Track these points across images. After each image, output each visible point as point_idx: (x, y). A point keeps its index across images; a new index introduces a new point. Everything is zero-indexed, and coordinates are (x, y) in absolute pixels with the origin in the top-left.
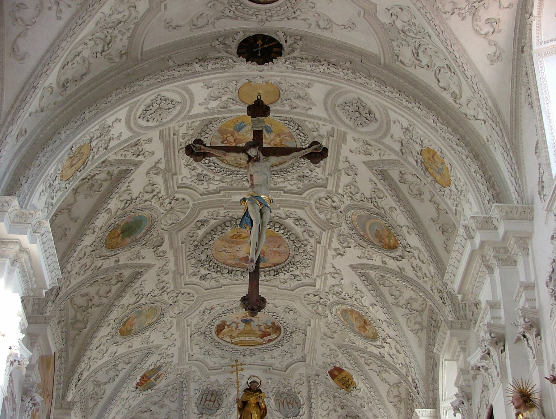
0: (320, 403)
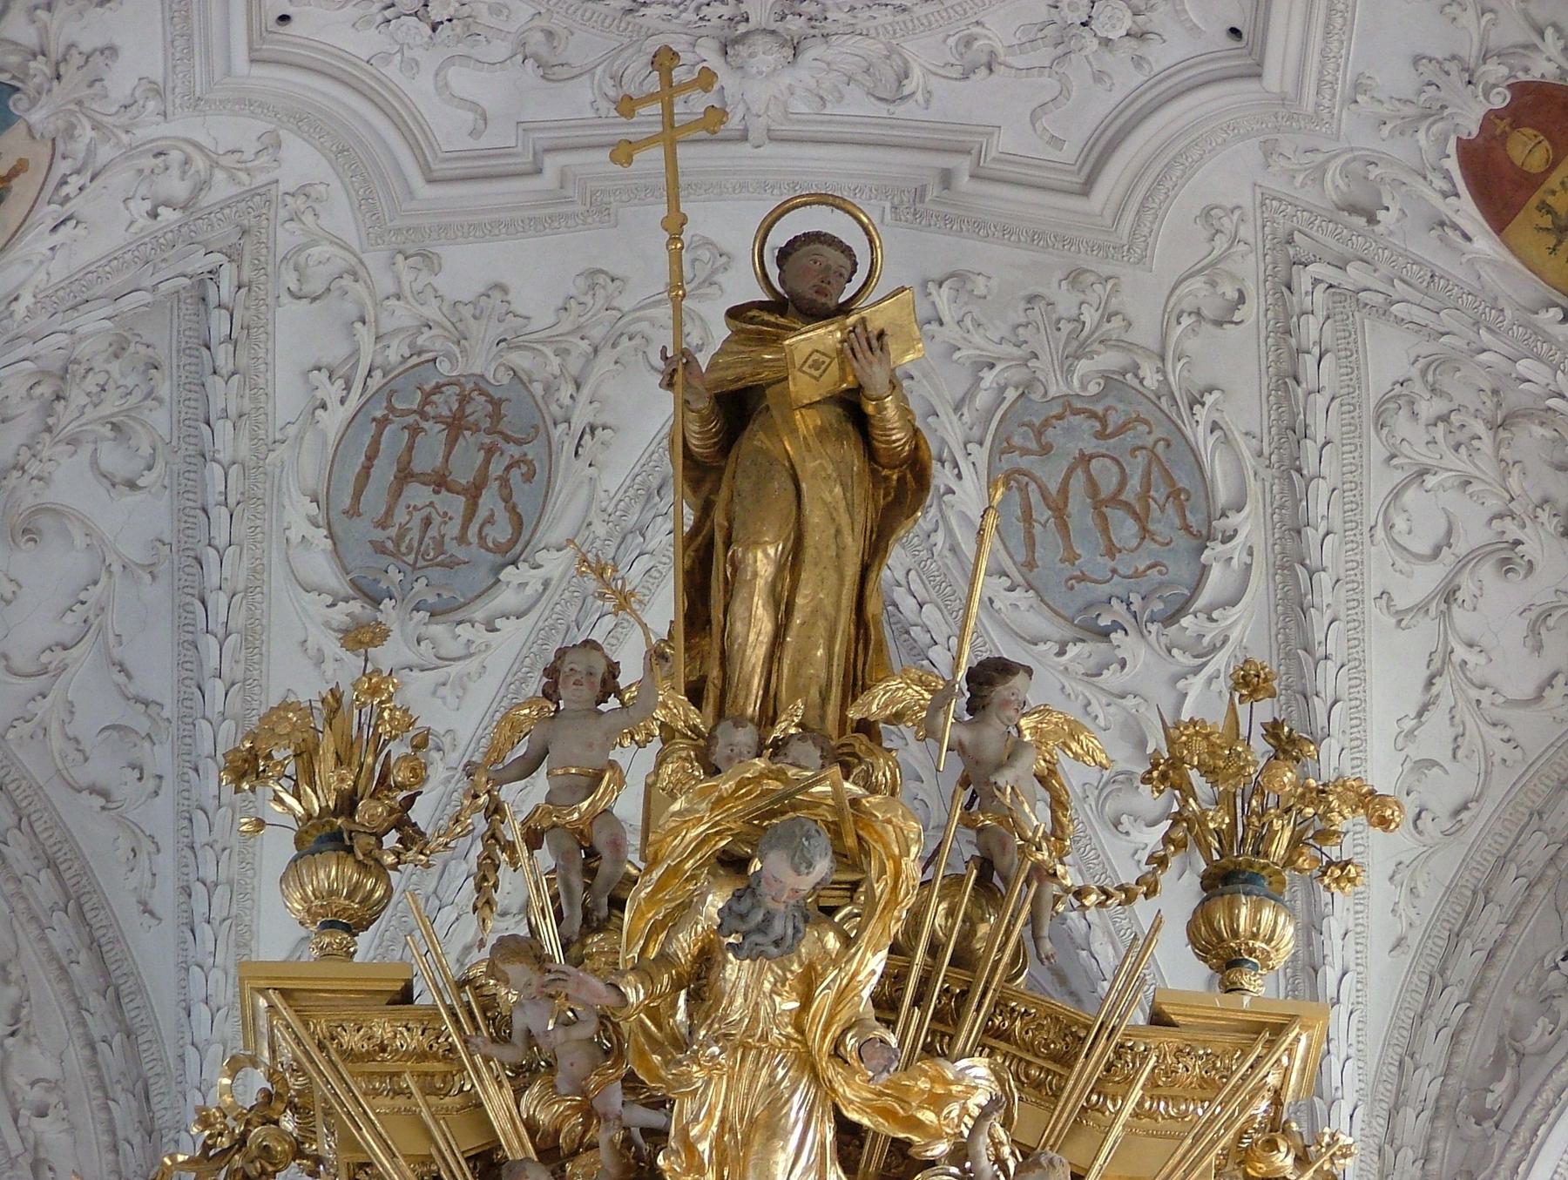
0: (1379, 484)
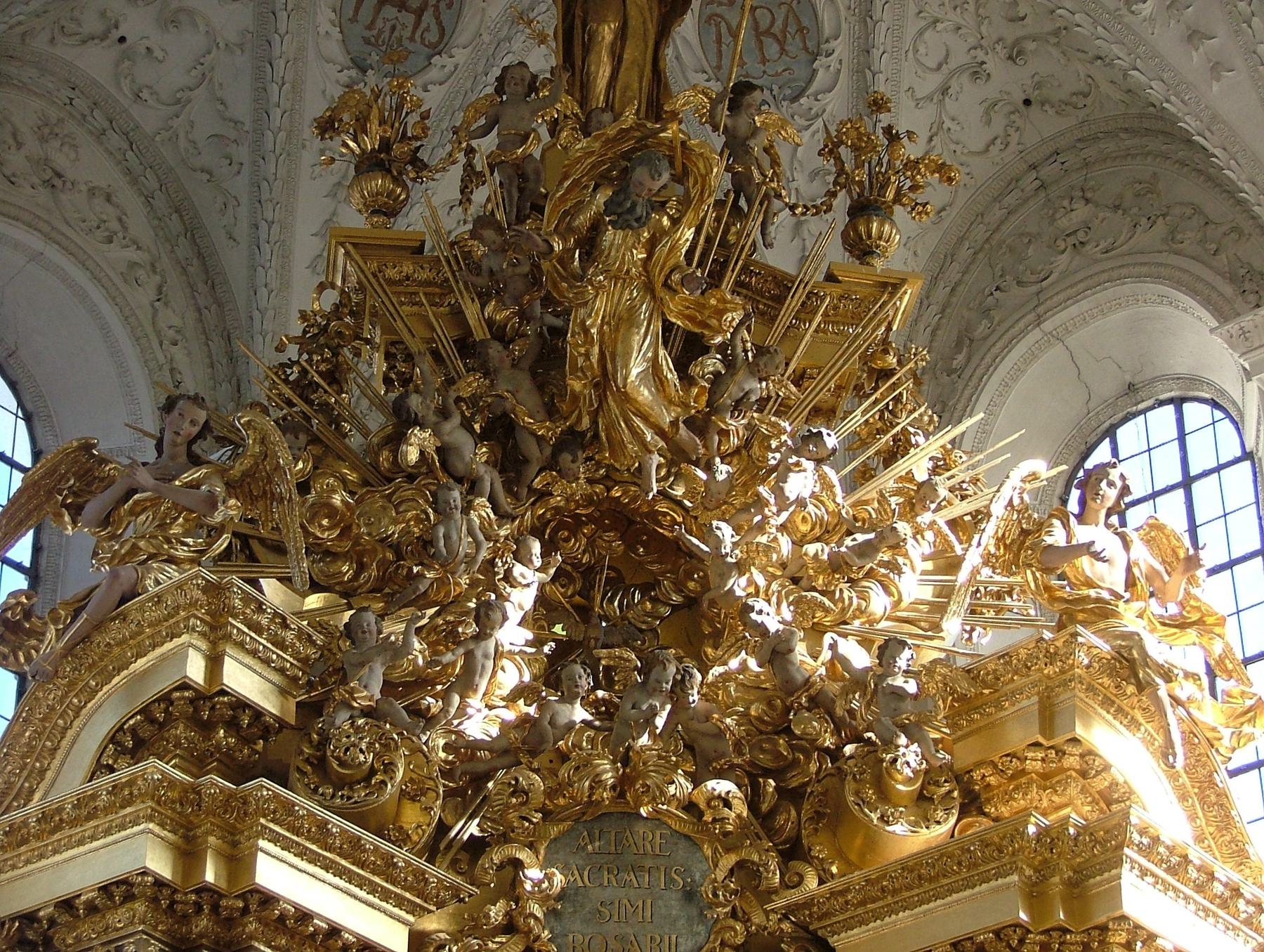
0: (912, 28)
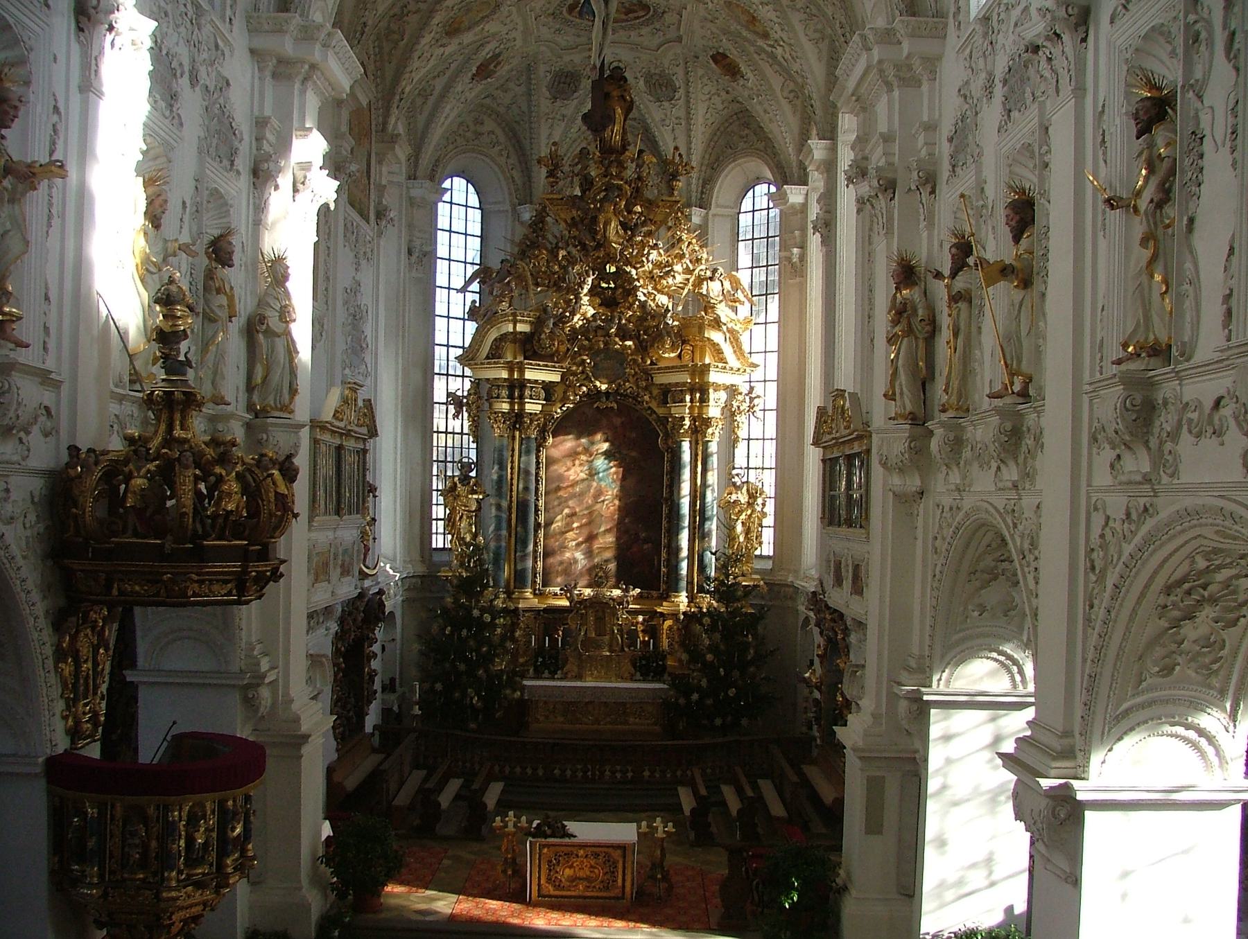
0: (700, 86)
